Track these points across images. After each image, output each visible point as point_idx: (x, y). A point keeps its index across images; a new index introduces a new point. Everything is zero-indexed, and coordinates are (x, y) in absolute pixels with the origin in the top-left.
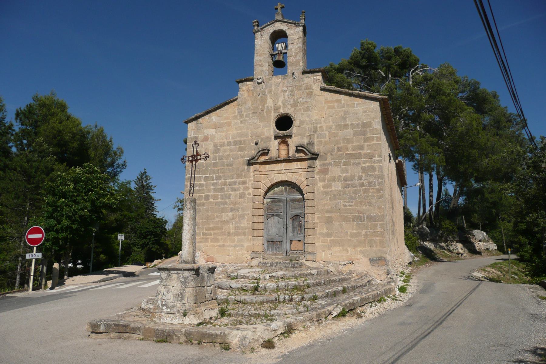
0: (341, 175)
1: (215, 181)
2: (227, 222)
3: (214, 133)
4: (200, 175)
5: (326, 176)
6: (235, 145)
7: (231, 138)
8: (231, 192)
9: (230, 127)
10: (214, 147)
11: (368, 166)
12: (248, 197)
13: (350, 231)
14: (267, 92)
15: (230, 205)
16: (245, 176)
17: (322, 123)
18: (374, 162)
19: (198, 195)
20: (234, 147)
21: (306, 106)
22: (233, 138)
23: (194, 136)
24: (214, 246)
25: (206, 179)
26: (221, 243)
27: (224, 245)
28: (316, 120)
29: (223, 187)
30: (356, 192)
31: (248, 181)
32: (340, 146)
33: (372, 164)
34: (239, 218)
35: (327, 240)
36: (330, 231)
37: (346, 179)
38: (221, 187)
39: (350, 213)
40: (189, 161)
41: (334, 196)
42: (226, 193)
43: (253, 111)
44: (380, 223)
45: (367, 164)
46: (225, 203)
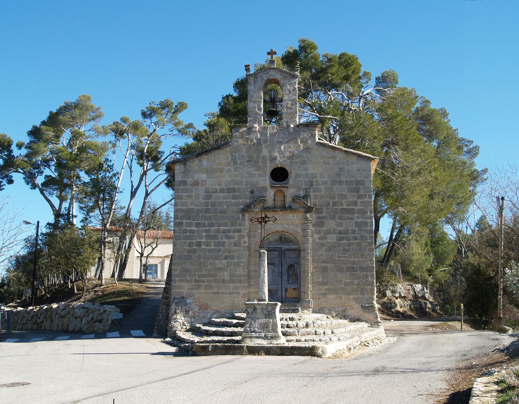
0: (336, 228)
1: (208, 228)
2: (221, 269)
3: (205, 179)
4: (191, 221)
5: (322, 229)
6: (229, 193)
7: (224, 184)
8: (225, 240)
9: (223, 173)
10: (206, 193)
11: (361, 222)
12: (244, 246)
13: (344, 280)
14: (262, 141)
15: (224, 252)
16: (240, 225)
17: (318, 177)
18: (366, 218)
19: (188, 241)
20: (228, 194)
21: (302, 159)
22: (226, 185)
23: (183, 179)
24: (208, 293)
25: (197, 225)
26: (215, 290)
27: (219, 292)
28: (312, 174)
29: (216, 234)
30: (349, 245)
31: (243, 230)
32: (334, 201)
33: (365, 220)
34: (234, 266)
35: (323, 288)
36: (325, 280)
37: (340, 232)
38: (214, 234)
39: (344, 264)
40: (258, 221)
41: (329, 248)
42: (220, 240)
43: (247, 159)
44: (371, 273)
45: (360, 220)
46: (219, 250)
